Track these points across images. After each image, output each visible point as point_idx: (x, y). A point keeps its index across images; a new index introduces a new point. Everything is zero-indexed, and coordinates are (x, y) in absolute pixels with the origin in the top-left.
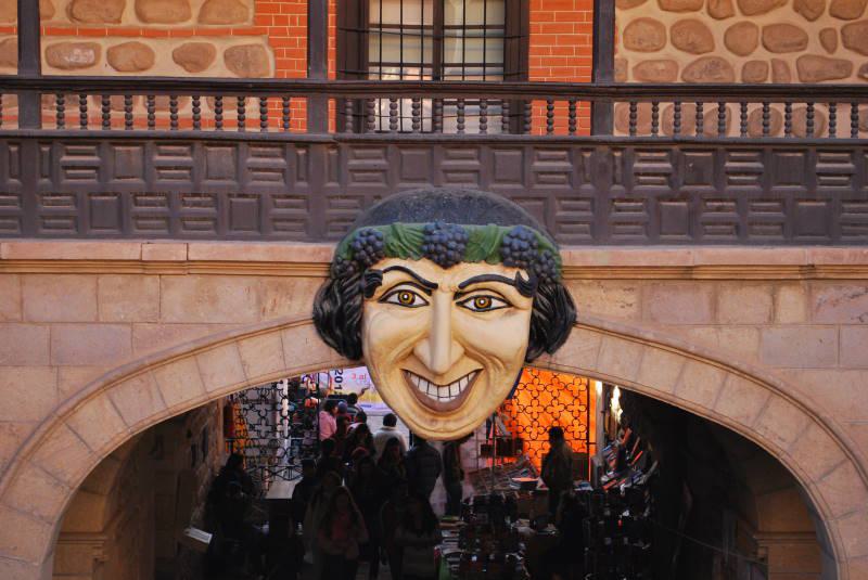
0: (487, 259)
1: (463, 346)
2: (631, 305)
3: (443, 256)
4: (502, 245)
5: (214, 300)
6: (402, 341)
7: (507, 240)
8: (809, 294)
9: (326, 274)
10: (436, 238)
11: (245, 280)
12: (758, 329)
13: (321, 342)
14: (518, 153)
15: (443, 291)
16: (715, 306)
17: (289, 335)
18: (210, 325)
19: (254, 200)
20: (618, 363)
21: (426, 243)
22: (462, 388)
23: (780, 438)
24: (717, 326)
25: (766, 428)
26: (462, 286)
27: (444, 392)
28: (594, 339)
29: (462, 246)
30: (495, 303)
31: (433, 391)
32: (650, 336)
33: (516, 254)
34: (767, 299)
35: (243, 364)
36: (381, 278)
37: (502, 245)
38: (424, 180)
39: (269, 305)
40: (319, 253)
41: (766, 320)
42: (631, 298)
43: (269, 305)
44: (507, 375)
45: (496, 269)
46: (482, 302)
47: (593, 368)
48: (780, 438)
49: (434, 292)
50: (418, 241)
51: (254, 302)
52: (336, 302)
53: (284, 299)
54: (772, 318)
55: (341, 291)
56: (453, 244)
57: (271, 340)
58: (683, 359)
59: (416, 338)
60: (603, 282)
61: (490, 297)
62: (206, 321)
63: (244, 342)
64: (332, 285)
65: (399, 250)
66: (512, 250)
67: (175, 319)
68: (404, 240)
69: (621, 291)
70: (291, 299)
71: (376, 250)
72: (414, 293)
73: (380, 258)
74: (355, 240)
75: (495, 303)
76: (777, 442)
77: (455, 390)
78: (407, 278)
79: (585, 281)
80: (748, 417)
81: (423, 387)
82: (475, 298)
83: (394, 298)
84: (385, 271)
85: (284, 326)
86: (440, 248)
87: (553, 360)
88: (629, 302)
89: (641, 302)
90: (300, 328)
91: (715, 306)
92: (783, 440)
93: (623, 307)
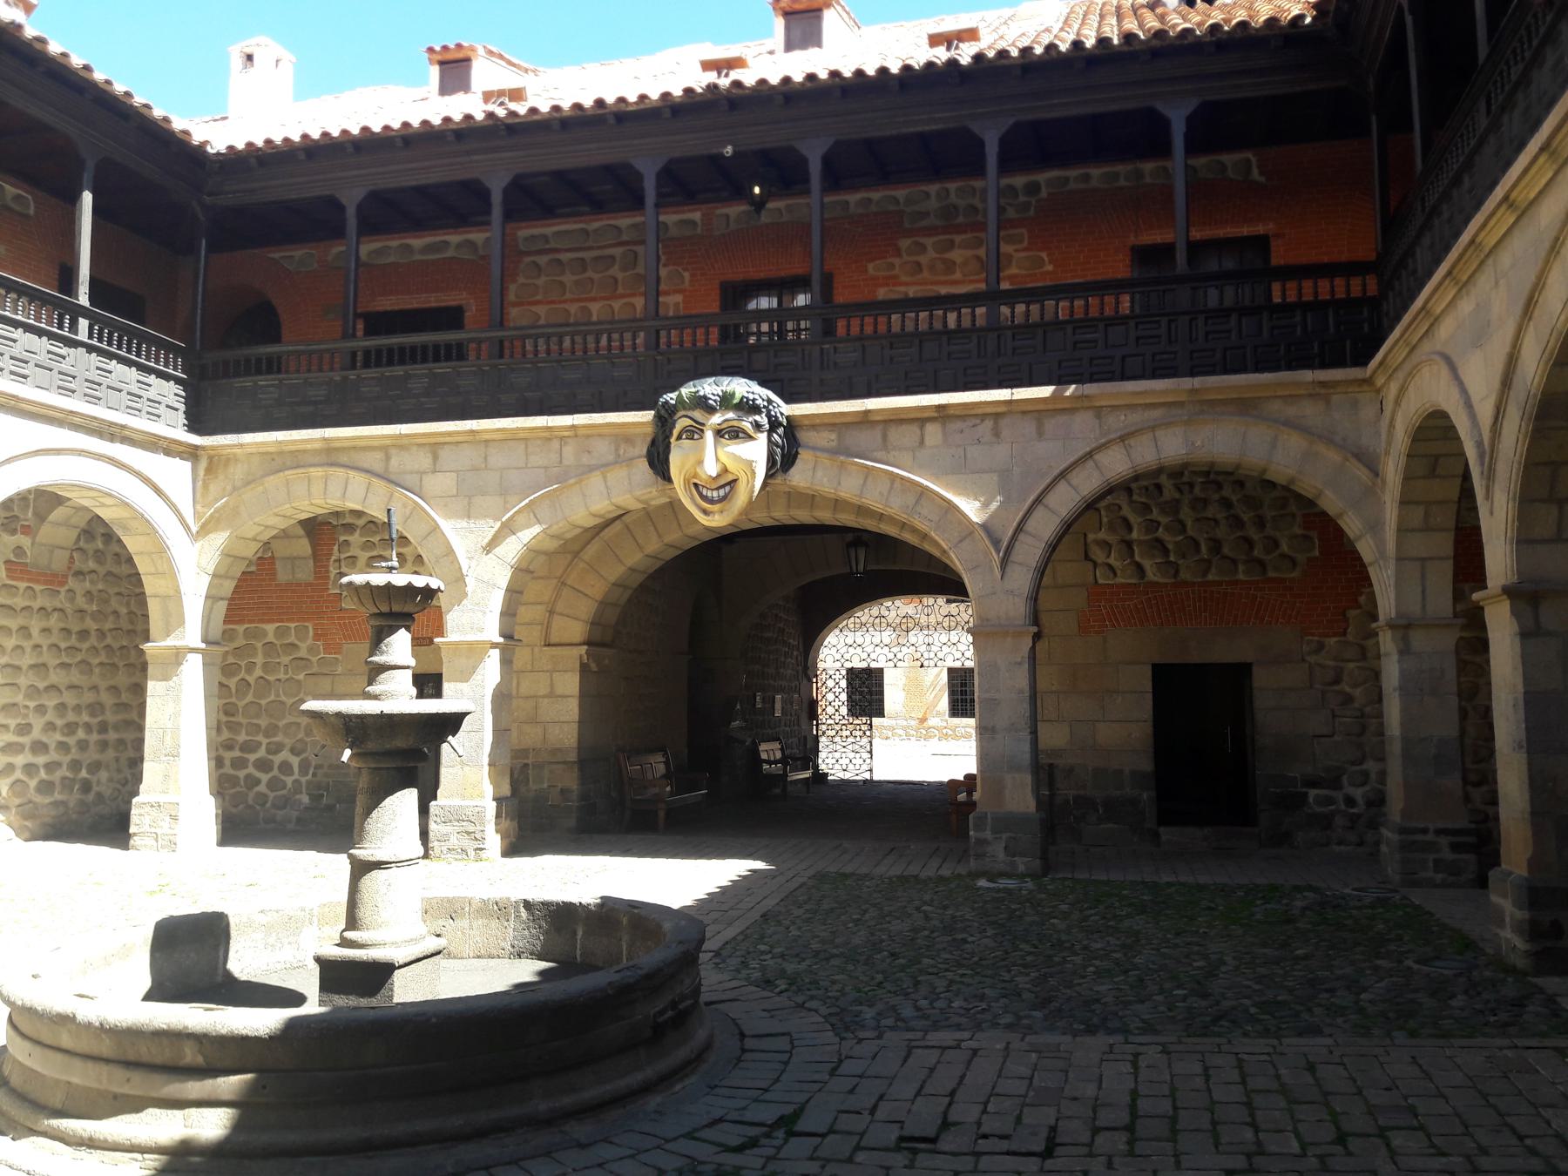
7: (746, 395)
8: (944, 425)
13: (651, 471)
16: (885, 437)
27: (715, 494)
34: (918, 432)
39: (622, 452)
42: (833, 436)
54: (922, 442)
61: (737, 432)
73: (675, 414)
75: (741, 435)
77: (722, 492)
78: (690, 422)
82: (728, 432)
91: (885, 437)
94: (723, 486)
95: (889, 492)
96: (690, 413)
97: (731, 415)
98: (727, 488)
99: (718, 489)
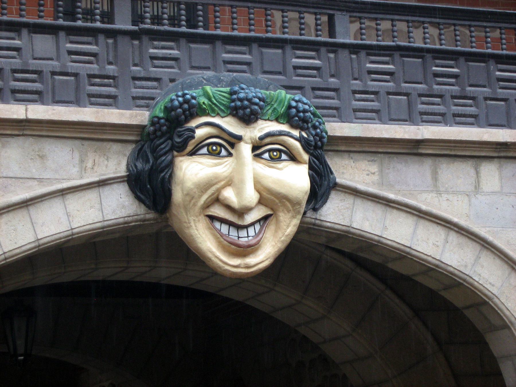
0: (277, 120)
2: (374, 173)
3: (249, 110)
4: (290, 107)
5: (42, 157)
6: (214, 185)
7: (294, 104)
9: (138, 138)
10: (242, 95)
11: (70, 142)
12: (467, 195)
14: (280, 51)
15: (246, 143)
17: (106, 191)
18: (40, 180)
19: (73, 78)
20: (368, 220)
21: (233, 101)
22: (257, 232)
23: (490, 283)
24: (439, 193)
25: (480, 275)
26: (261, 138)
27: (243, 233)
28: (349, 200)
29: (262, 103)
30: (284, 157)
31: (233, 233)
32: (392, 196)
33: (301, 114)
35: (68, 215)
36: (194, 132)
37: (290, 107)
38: (208, 68)
39: (90, 164)
40: (136, 116)
41: (473, 189)
42: (374, 168)
43: (90, 164)
44: (294, 217)
45: (284, 128)
46: (275, 154)
47: (349, 225)
48: (490, 283)
49: (237, 146)
50: (225, 101)
51: (77, 162)
52: (148, 161)
53: (101, 160)
54: (477, 187)
55: (154, 151)
56: (257, 100)
57: (92, 195)
58: (415, 218)
59: (223, 183)
60: (352, 155)
61: (280, 151)
62: (37, 177)
63: (69, 196)
64: (143, 146)
65: (208, 108)
66: (298, 111)
67: (11, 175)
68: (213, 100)
69: (367, 163)
71: (192, 106)
72: (221, 145)
74: (172, 100)
76: (488, 286)
80: (466, 266)
81: (224, 229)
82: (269, 151)
83: (205, 150)
84: (198, 127)
85: (102, 183)
86: (246, 103)
87: (318, 216)
88: (373, 172)
89: (381, 171)
92: (493, 285)
93: (368, 175)
94: (253, 224)
95: (444, 246)
96: (217, 120)
97: (274, 127)
98: (258, 227)
99: (246, 227)
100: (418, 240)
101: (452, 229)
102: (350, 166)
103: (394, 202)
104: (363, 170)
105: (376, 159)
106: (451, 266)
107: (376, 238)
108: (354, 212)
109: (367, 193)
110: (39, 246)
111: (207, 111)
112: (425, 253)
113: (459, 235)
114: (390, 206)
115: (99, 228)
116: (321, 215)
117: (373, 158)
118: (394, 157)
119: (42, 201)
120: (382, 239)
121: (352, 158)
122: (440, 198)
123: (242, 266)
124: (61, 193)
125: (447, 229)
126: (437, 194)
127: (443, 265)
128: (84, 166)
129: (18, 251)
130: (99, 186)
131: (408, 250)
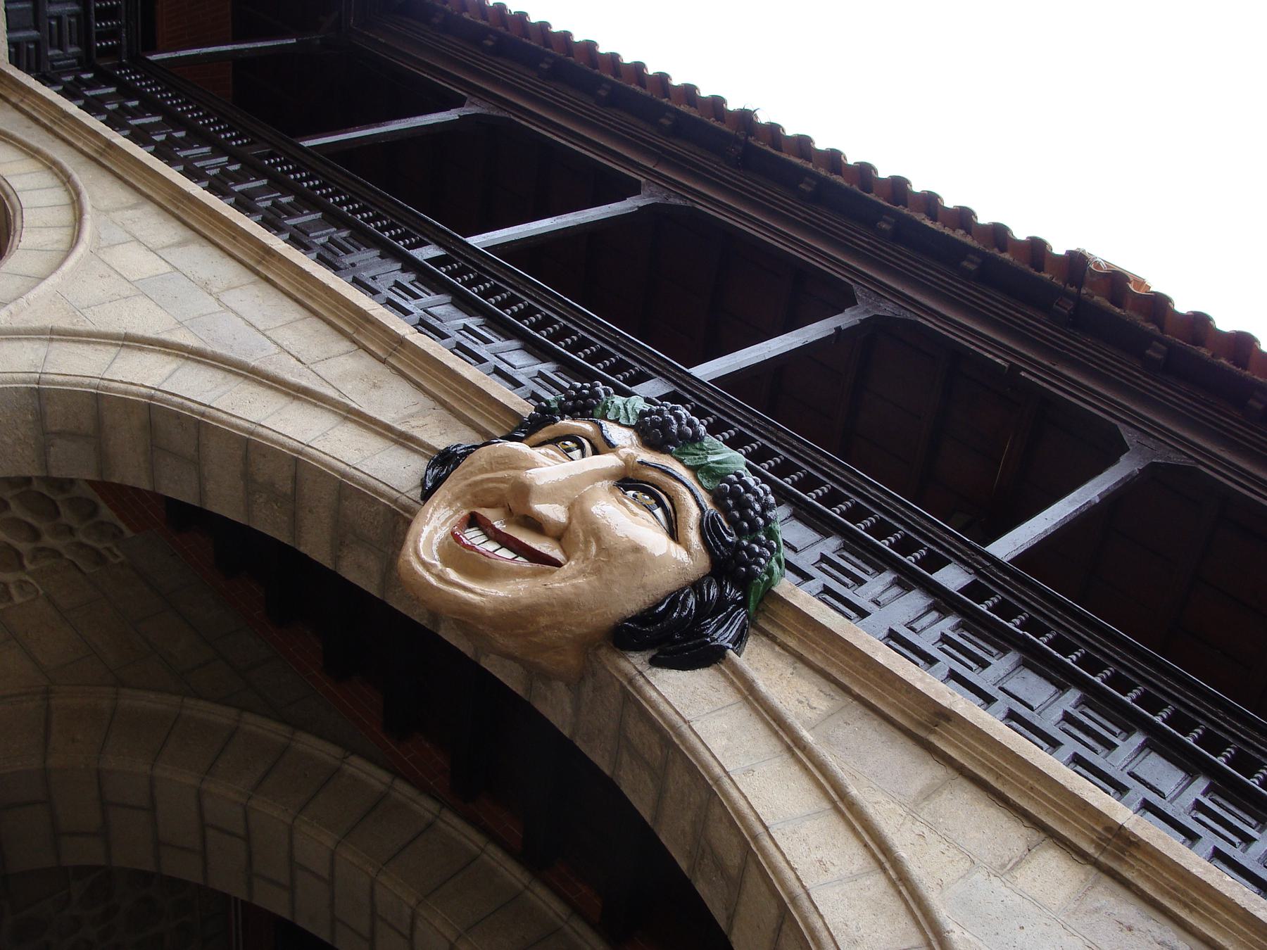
1: (570, 519)
47: (688, 718)
60: (799, 665)
70: (441, 434)
79: (777, 648)
88: (814, 706)
90: (416, 457)
91: (928, 794)
100: (795, 832)
101: (884, 870)
102: (779, 673)
103: (804, 747)
104: (797, 692)
105: (837, 698)
106: (821, 916)
107: (718, 770)
108: (717, 713)
109: (765, 703)
110: (252, 433)
111: (607, 411)
112: (789, 858)
113: (891, 891)
114: (793, 754)
115: (337, 471)
116: (654, 675)
117: (832, 694)
118: (876, 720)
119: (316, 405)
120: (726, 780)
121: (794, 668)
122: (909, 824)
123: (434, 571)
124: (345, 414)
125: (874, 865)
126: (908, 814)
127: (807, 904)
128: (408, 420)
129: (224, 416)
130: (396, 442)
131: (759, 829)
